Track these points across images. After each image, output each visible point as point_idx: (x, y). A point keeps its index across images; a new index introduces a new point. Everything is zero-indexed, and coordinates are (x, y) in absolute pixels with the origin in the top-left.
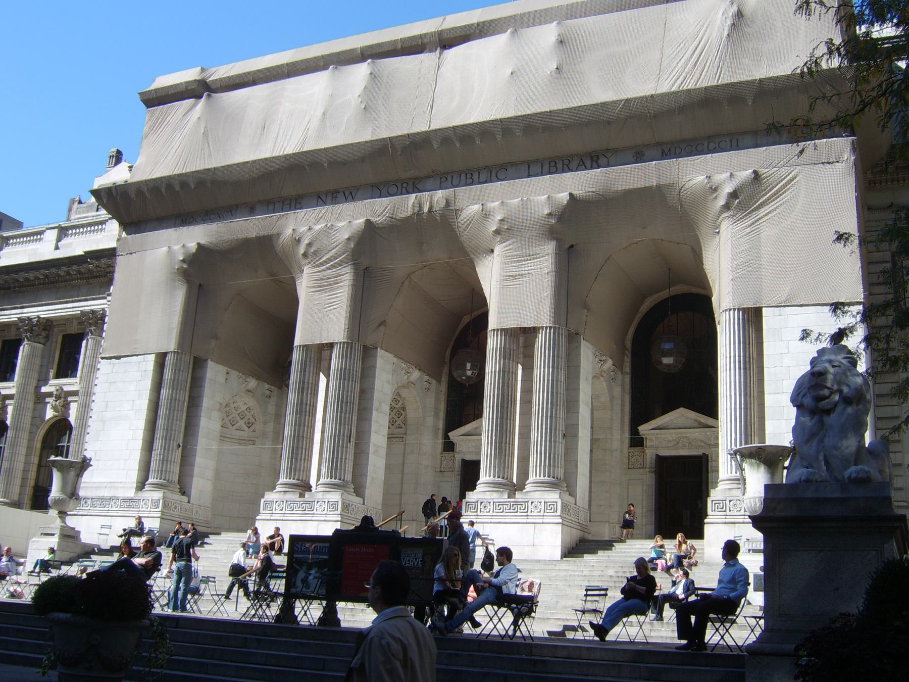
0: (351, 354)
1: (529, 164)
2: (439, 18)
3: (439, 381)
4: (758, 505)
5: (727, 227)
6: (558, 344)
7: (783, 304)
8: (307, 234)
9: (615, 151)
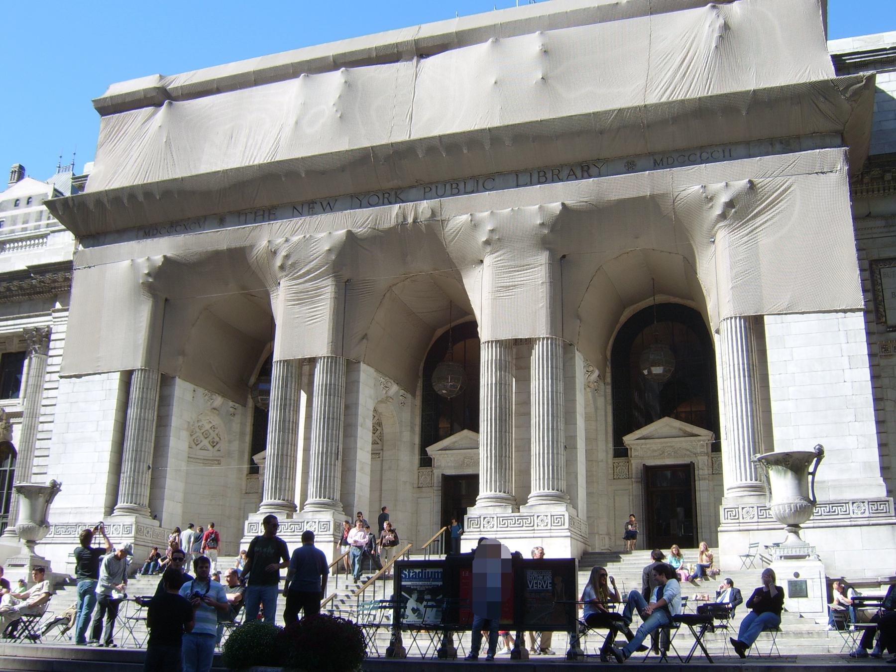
0: (335, 369)
1: (517, 173)
2: (414, 27)
3: (414, 395)
4: (787, 511)
5: (723, 236)
6: (556, 355)
7: (785, 312)
8: (284, 245)
9: (606, 161)
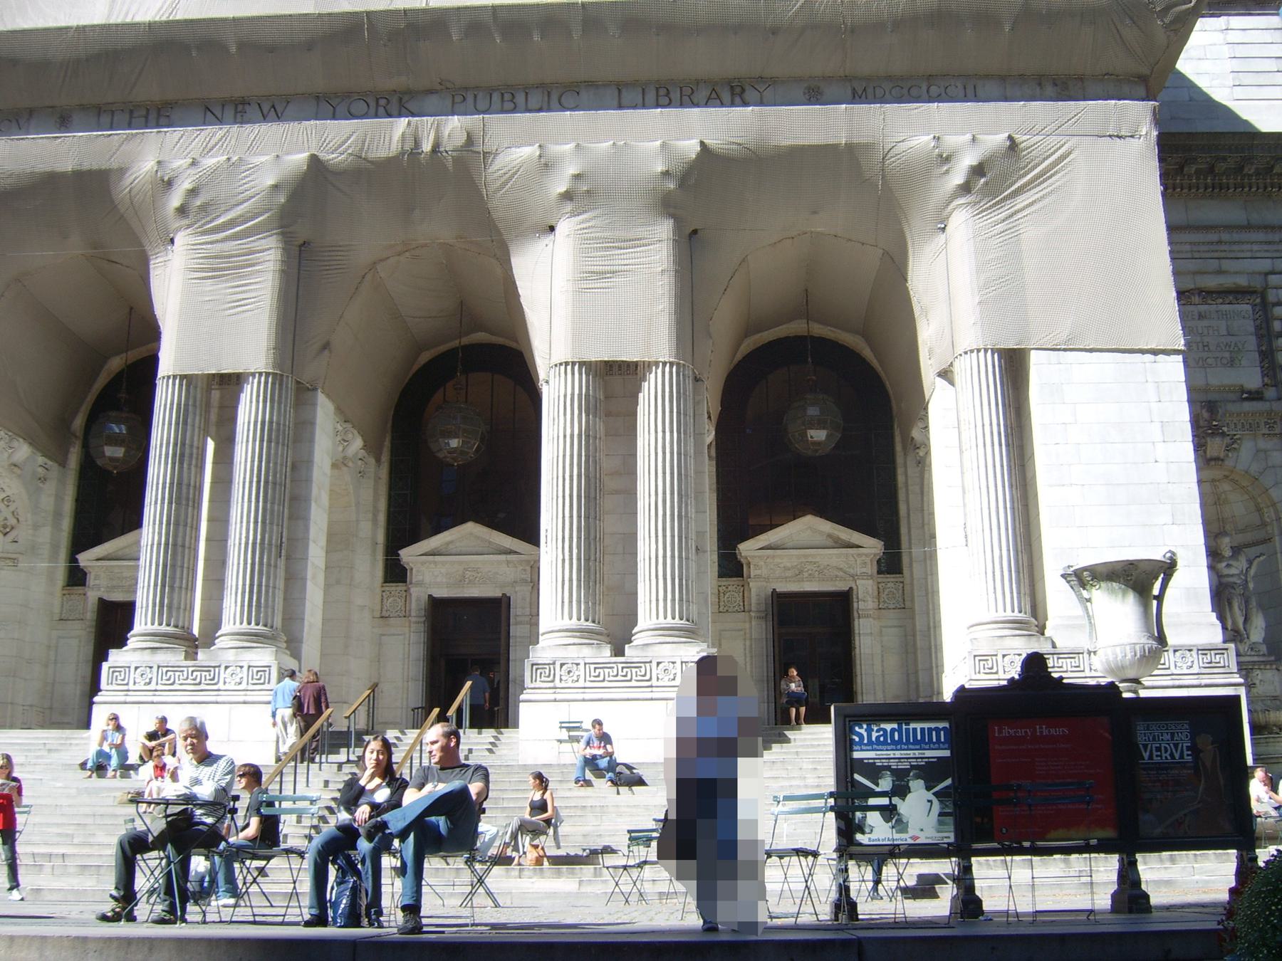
0: (280, 396)
1: (620, 87)
4: (1129, 656)
5: (961, 220)
6: (684, 394)
7: (1063, 347)
8: (189, 171)
9: (773, 82)
